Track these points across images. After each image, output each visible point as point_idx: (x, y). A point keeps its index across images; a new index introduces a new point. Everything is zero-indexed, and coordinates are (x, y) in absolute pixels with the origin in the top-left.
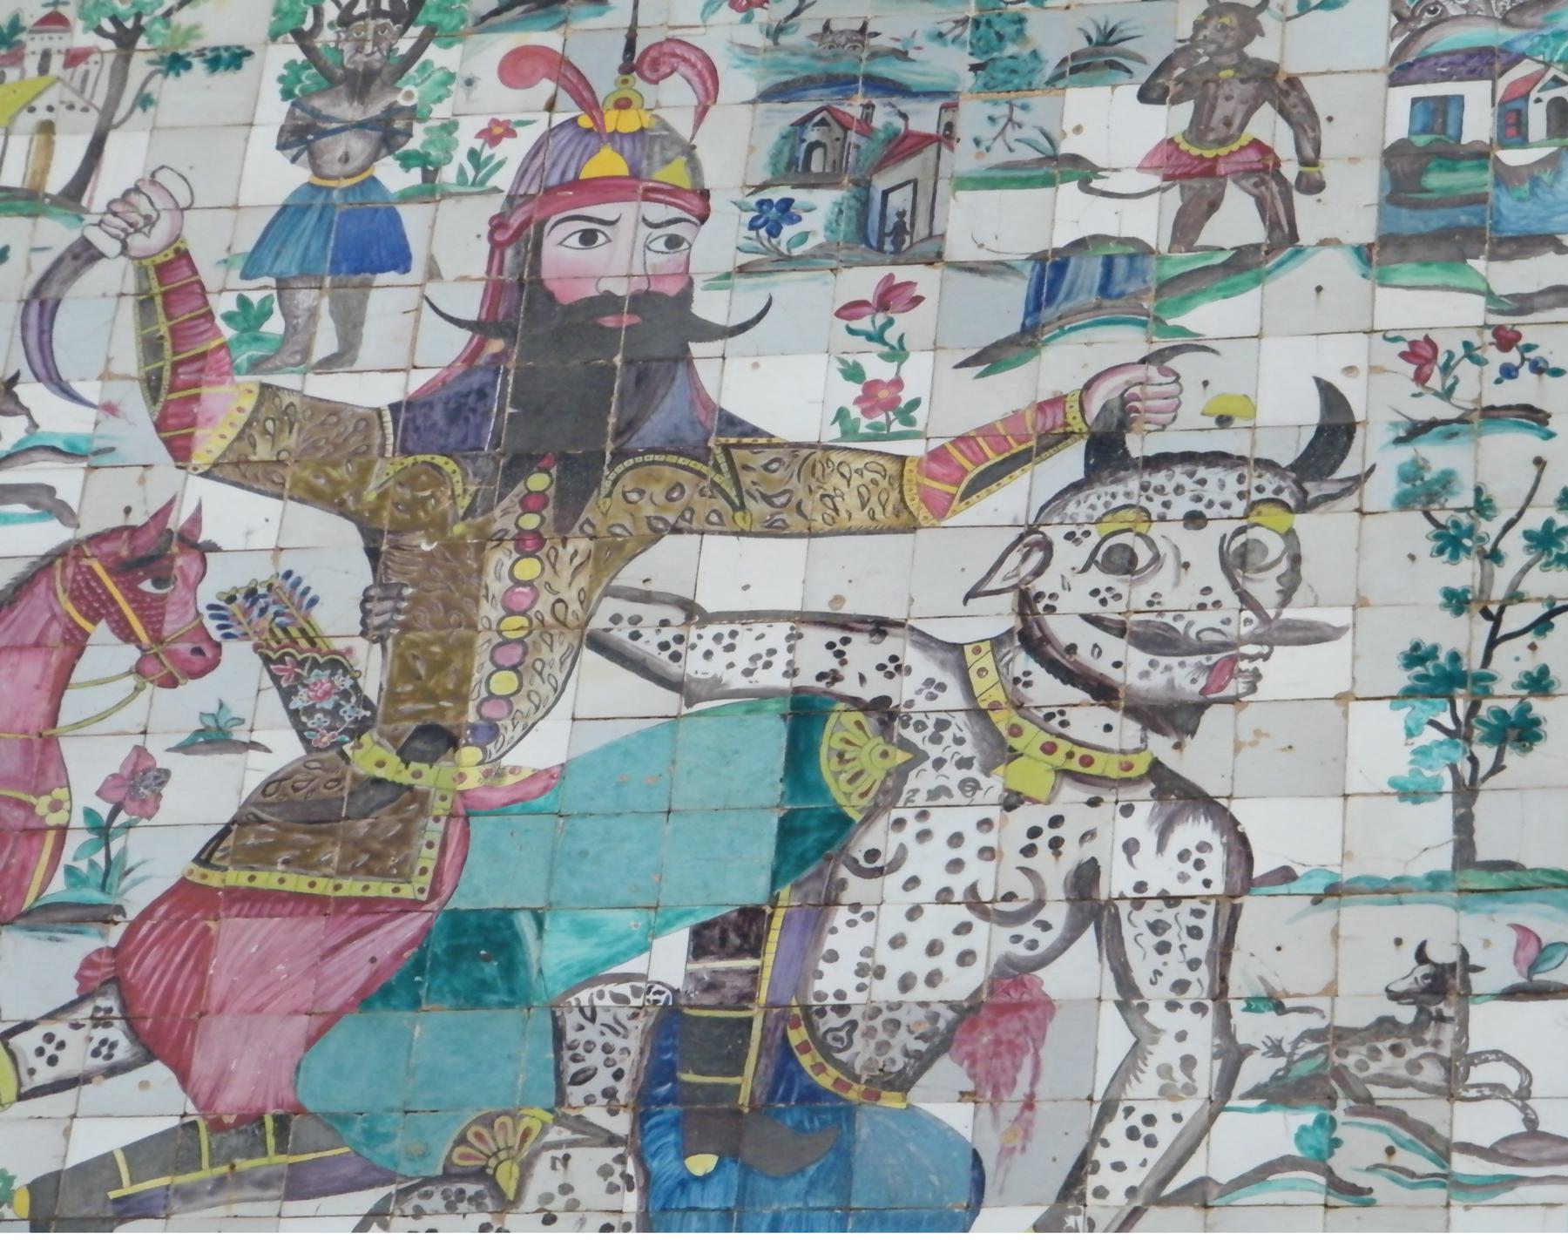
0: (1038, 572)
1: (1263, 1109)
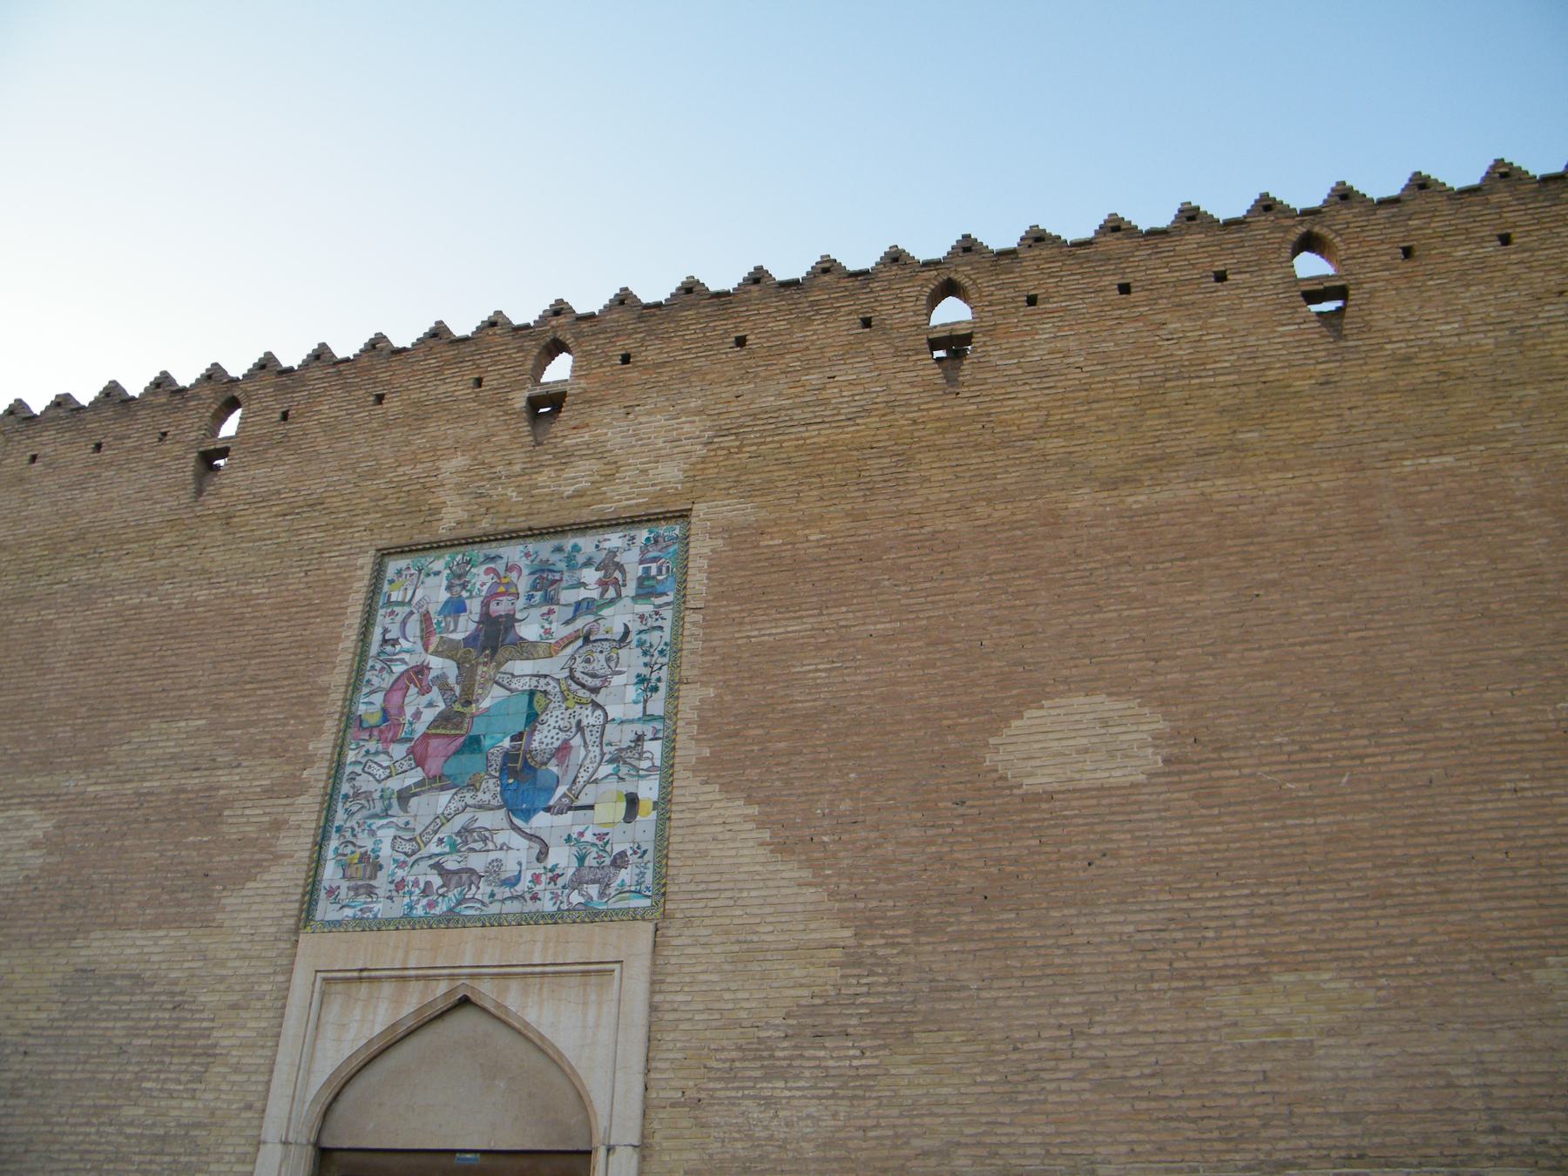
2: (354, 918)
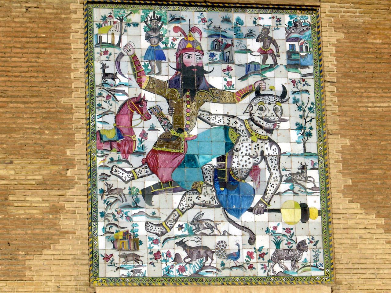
2: (129, 276)
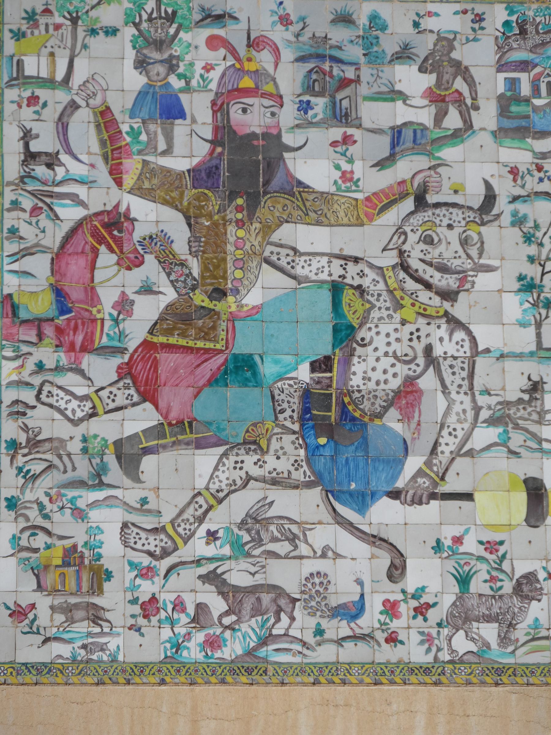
0: (404, 243)
1: (487, 427)
2: (74, 660)
